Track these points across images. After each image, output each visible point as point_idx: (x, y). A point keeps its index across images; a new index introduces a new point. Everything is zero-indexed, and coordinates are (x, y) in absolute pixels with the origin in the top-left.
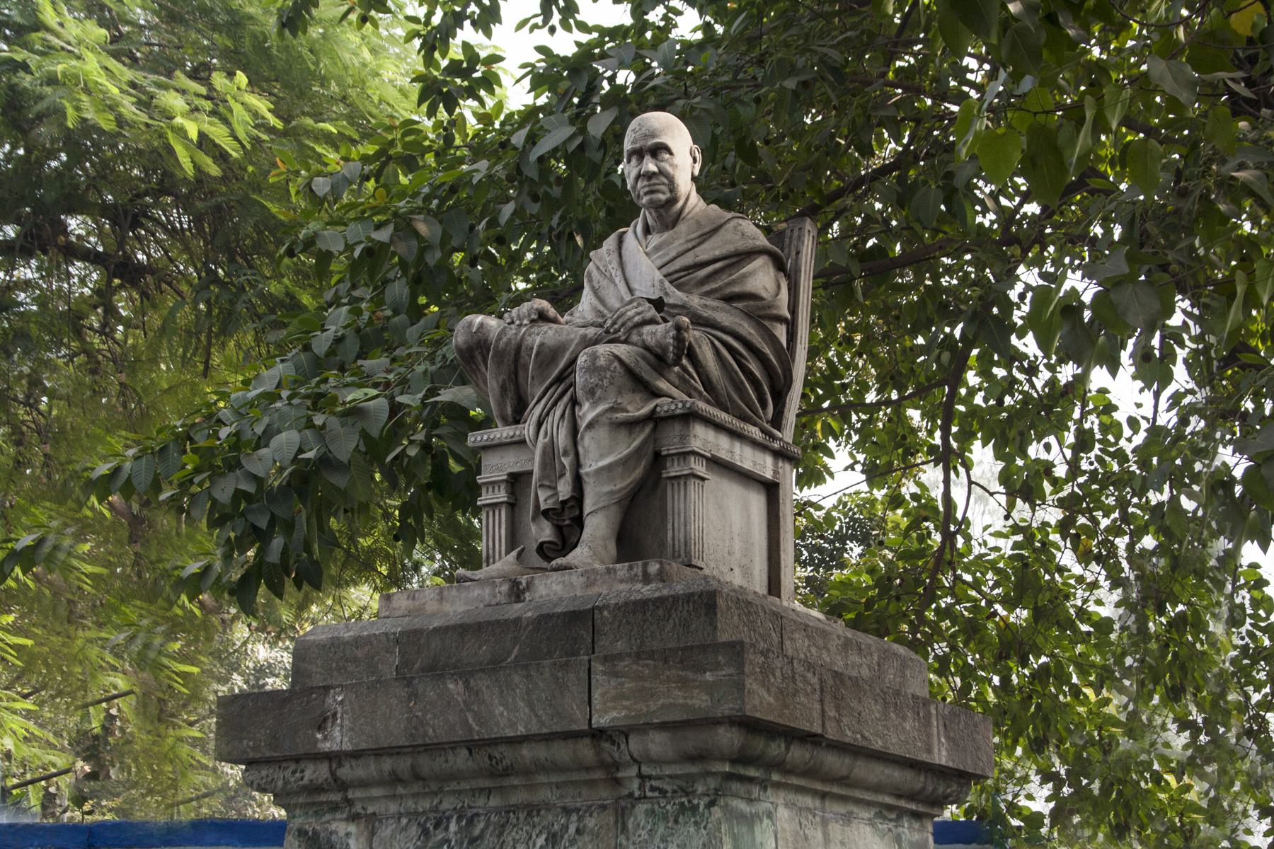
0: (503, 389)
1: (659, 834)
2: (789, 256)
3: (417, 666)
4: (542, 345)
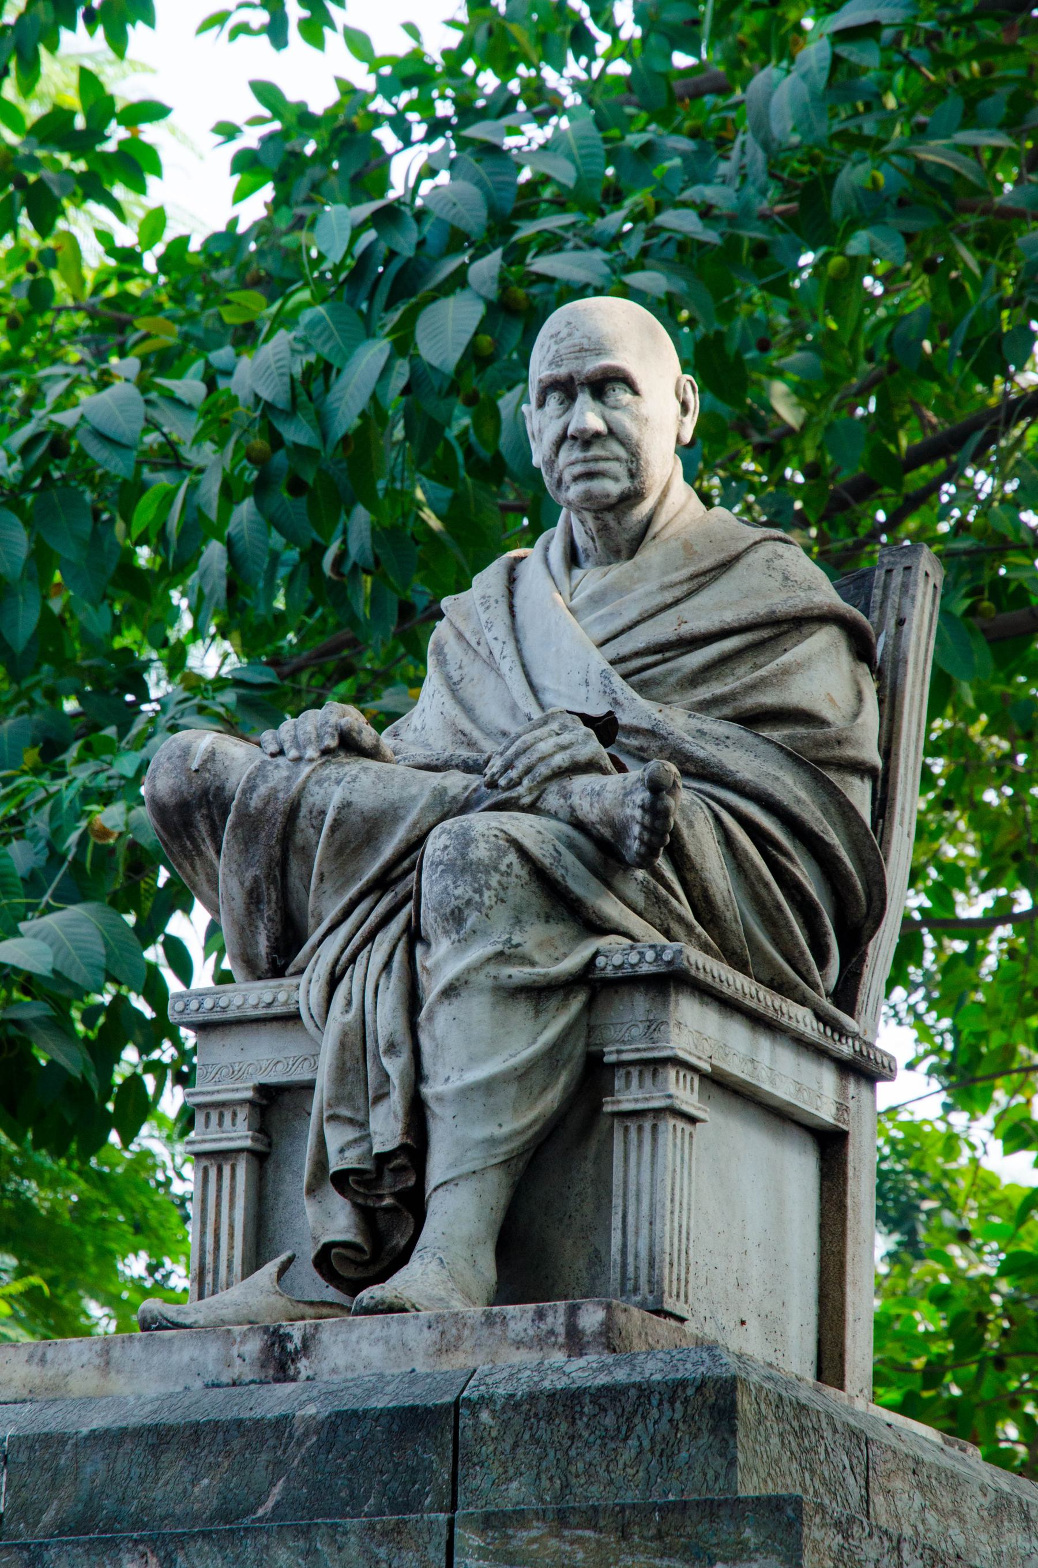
0: (254, 898)
2: (880, 626)
3: (47, 1518)
4: (346, 806)
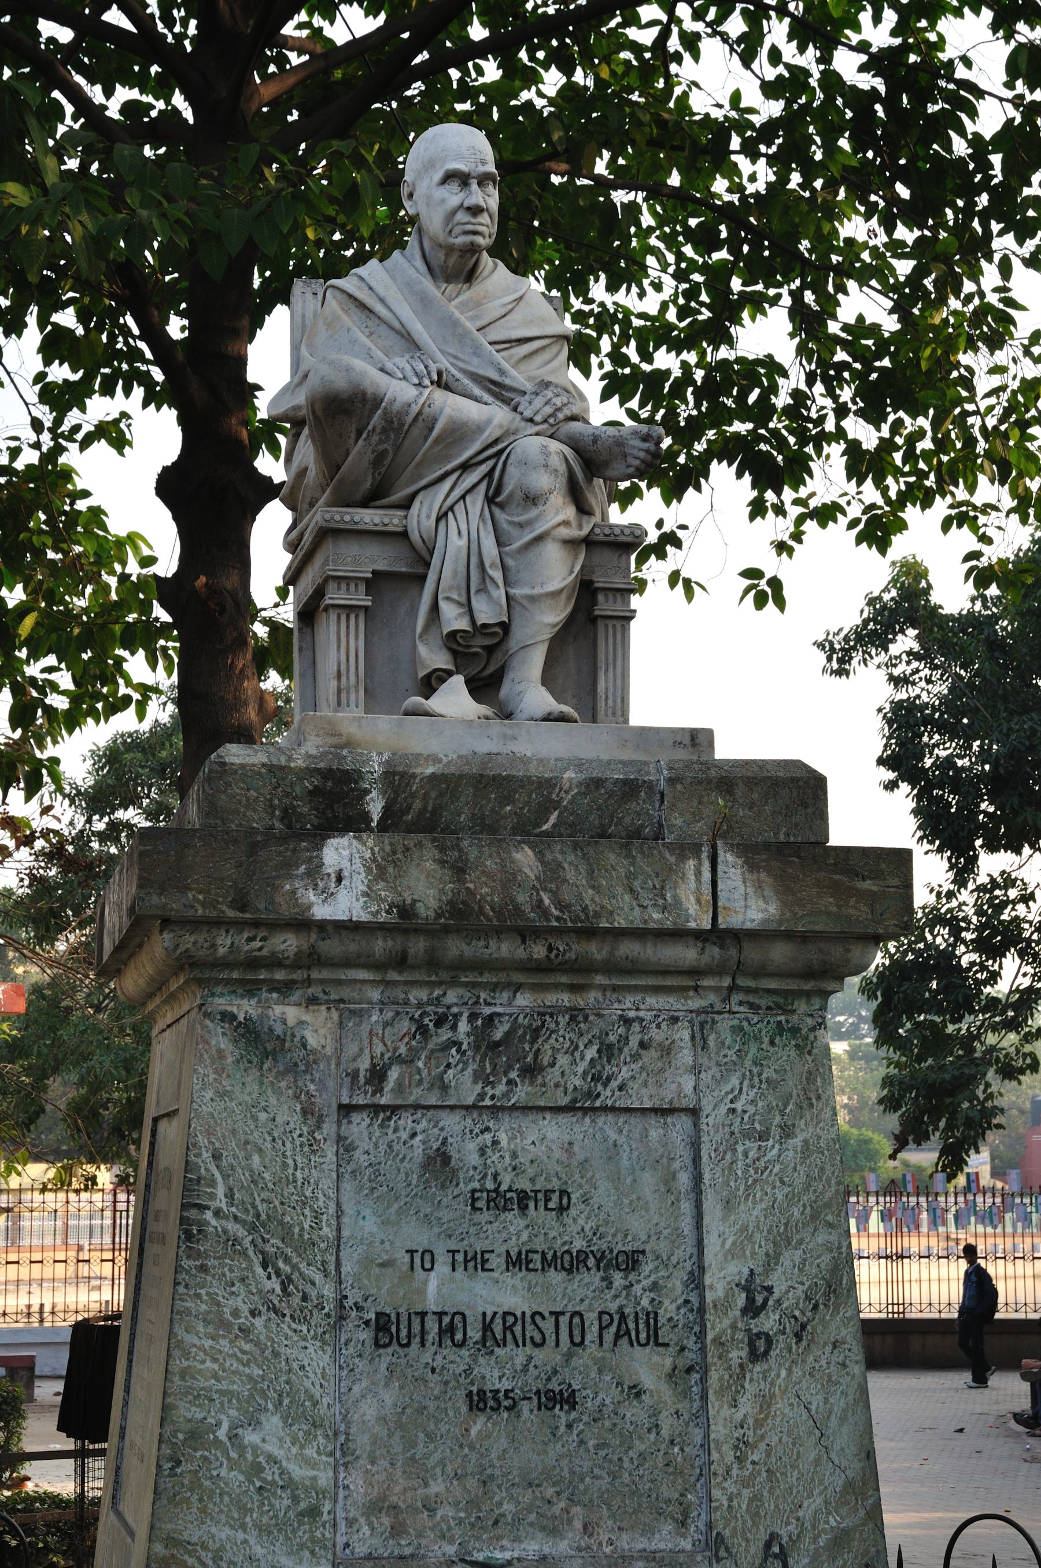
1: (750, 1056)
